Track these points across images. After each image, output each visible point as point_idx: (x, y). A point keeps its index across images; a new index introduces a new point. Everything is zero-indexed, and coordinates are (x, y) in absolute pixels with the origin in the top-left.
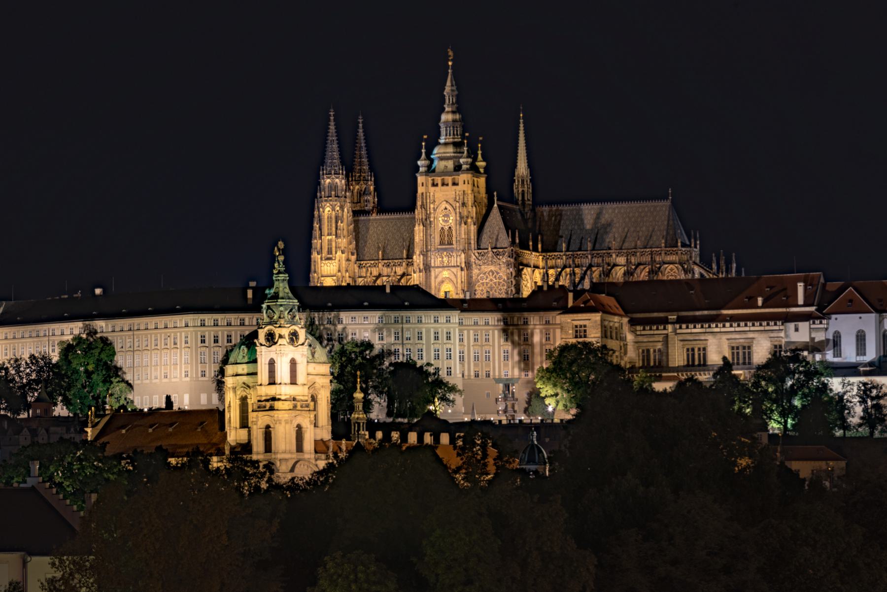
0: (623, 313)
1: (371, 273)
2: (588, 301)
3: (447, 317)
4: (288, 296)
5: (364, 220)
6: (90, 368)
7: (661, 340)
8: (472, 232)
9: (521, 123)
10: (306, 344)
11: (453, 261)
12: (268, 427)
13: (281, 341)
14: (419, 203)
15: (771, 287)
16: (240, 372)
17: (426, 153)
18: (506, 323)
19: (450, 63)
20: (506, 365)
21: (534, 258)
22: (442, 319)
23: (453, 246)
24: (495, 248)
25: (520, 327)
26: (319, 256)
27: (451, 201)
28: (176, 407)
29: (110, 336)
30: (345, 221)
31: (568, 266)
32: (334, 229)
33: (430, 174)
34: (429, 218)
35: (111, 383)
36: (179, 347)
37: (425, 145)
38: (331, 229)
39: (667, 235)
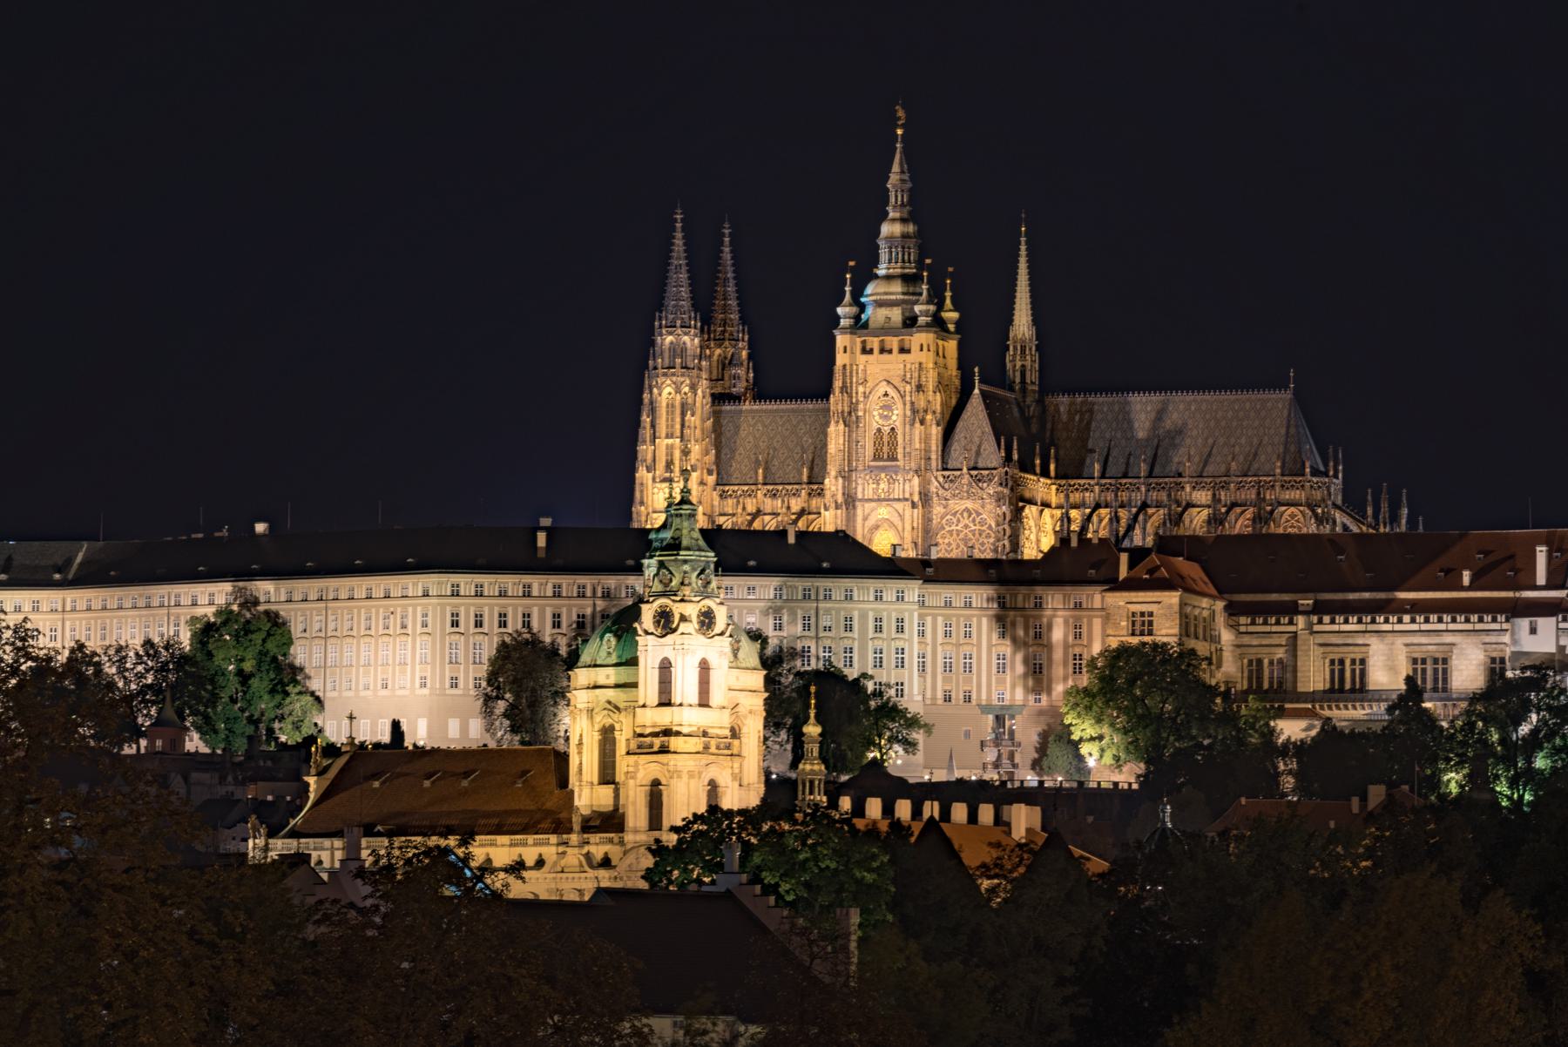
0: (1213, 591)
1: (744, 509)
2: (1158, 568)
3: (898, 592)
4: (698, 545)
5: (730, 411)
6: (248, 666)
7: (1284, 643)
8: (934, 437)
9: (1023, 243)
10: (728, 634)
11: (896, 491)
12: (656, 783)
13: (683, 627)
14: (837, 384)
15: (1486, 553)
16: (602, 681)
17: (852, 293)
18: (1002, 605)
19: (899, 132)
20: (1001, 682)
21: (1042, 488)
22: (889, 596)
24: (975, 468)
25: (1028, 613)
26: (650, 475)
27: (896, 382)
28: (408, 743)
29: (284, 610)
30: (699, 412)
31: (1103, 505)
32: (678, 426)
33: (859, 331)
34: (856, 410)
35: (287, 694)
36: (410, 632)
37: (851, 278)
38: (672, 426)
39: (1285, 453)
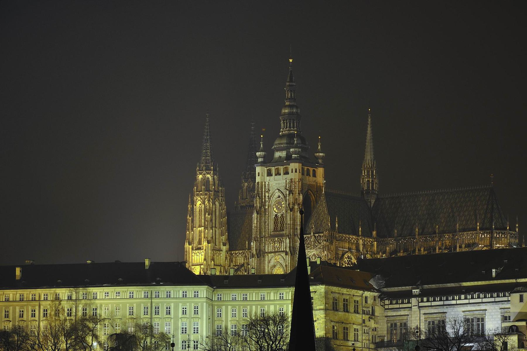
9: (369, 117)
11: (282, 247)
23: (284, 232)
26: (191, 247)
32: (203, 221)
33: (265, 164)
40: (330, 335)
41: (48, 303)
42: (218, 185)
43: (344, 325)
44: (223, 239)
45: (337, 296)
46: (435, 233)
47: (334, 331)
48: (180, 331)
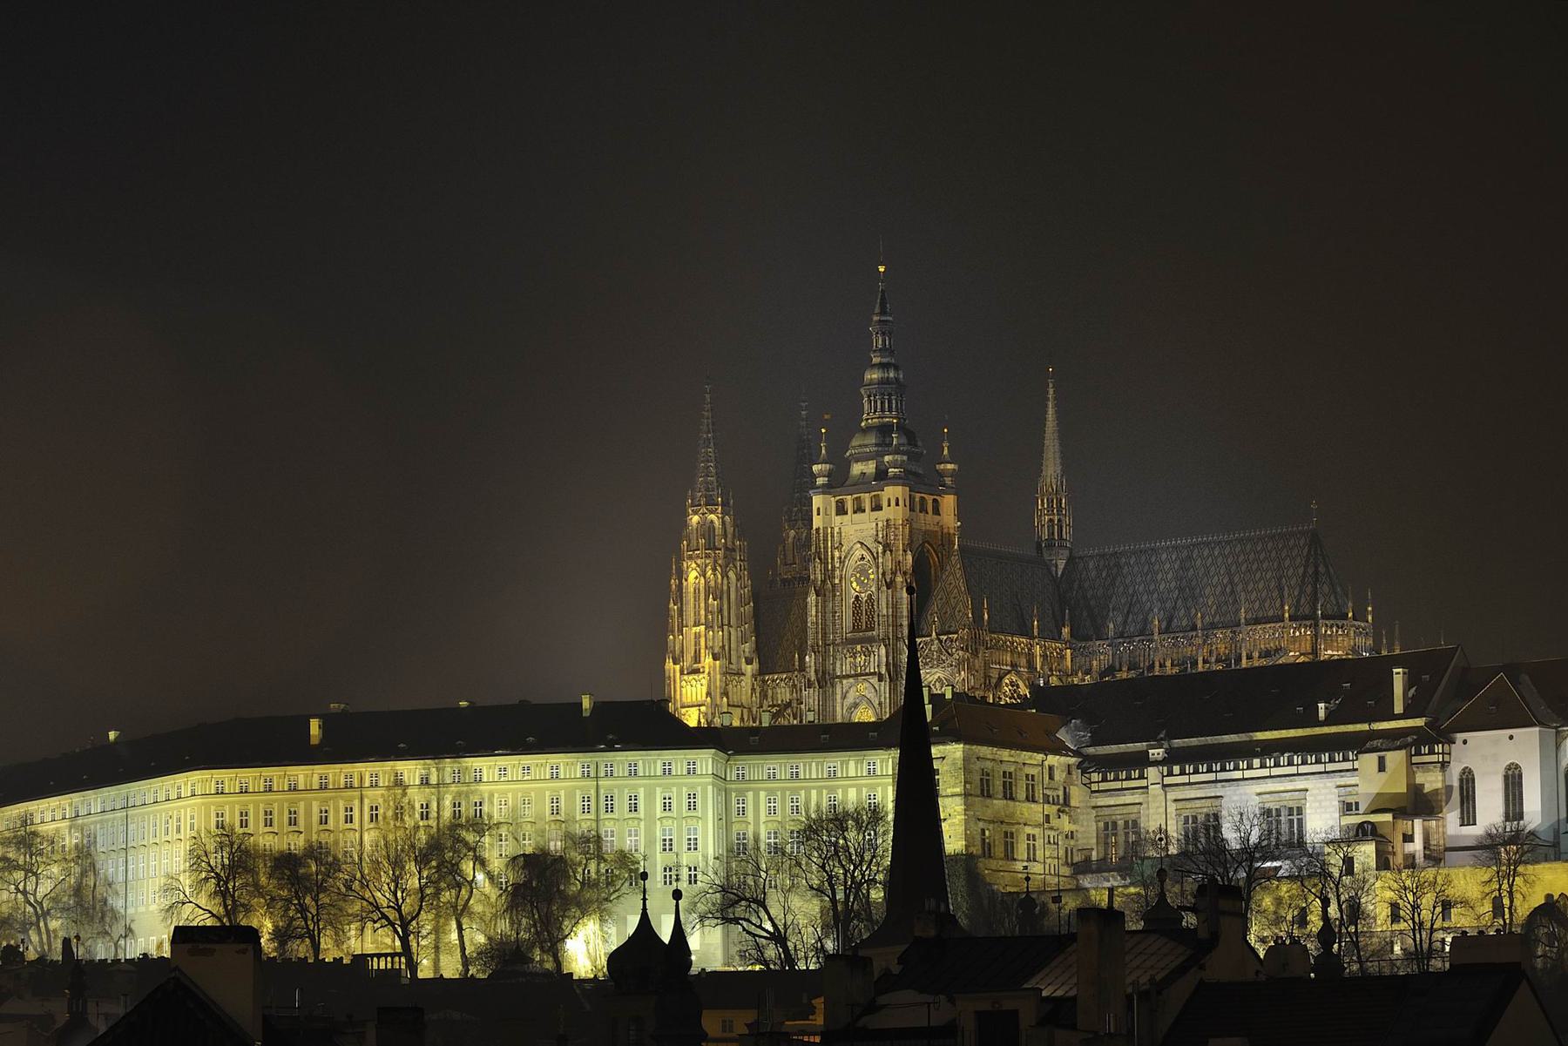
3: (689, 764)
9: (1051, 385)
11: (872, 663)
23: (874, 633)
26: (678, 667)
27: (870, 543)
32: (703, 612)
33: (832, 490)
36: (182, 838)
40: (977, 850)
41: (379, 792)
42: (734, 535)
43: (1005, 828)
44: (747, 650)
45: (989, 765)
46: (1194, 628)
47: (984, 840)
48: (659, 847)
